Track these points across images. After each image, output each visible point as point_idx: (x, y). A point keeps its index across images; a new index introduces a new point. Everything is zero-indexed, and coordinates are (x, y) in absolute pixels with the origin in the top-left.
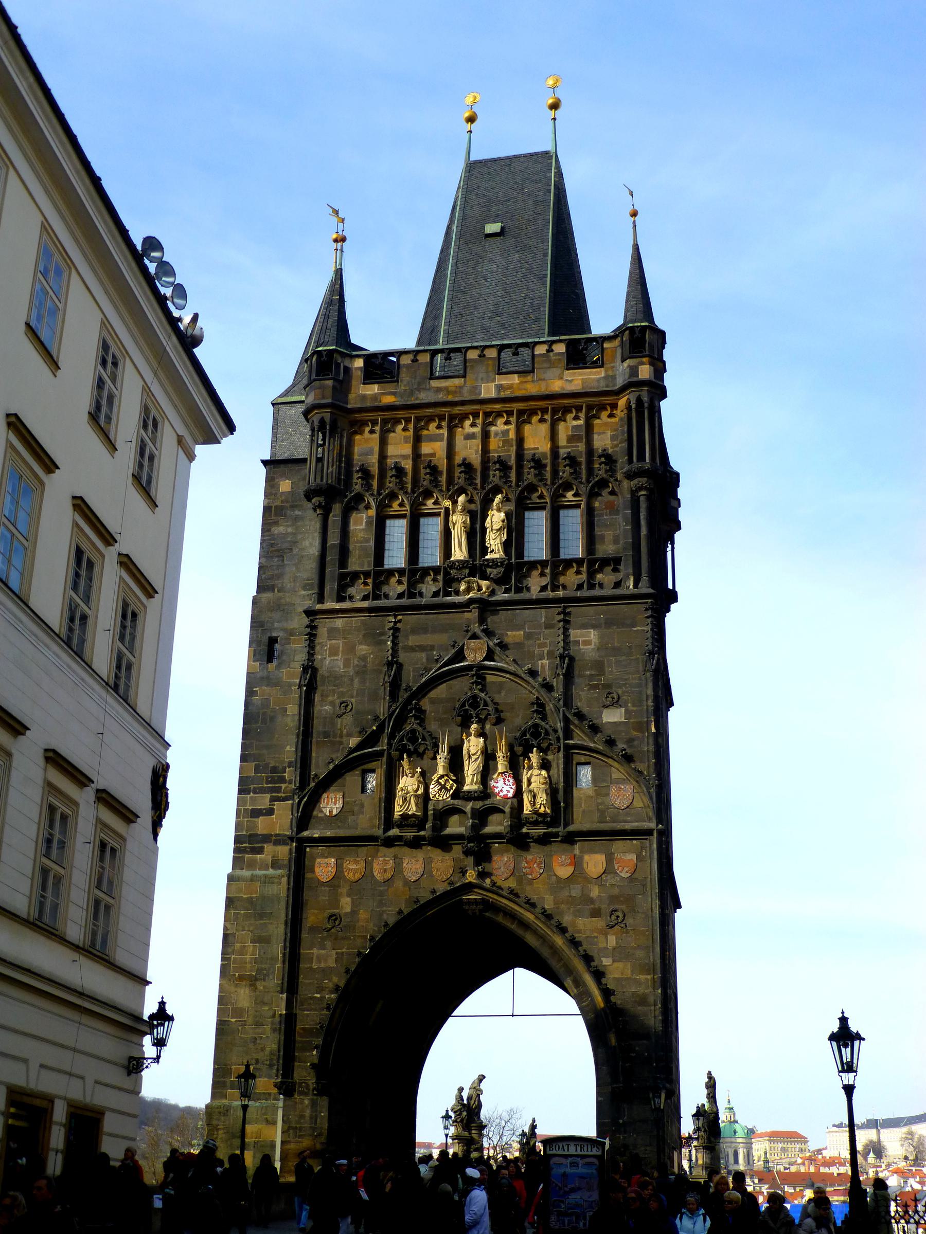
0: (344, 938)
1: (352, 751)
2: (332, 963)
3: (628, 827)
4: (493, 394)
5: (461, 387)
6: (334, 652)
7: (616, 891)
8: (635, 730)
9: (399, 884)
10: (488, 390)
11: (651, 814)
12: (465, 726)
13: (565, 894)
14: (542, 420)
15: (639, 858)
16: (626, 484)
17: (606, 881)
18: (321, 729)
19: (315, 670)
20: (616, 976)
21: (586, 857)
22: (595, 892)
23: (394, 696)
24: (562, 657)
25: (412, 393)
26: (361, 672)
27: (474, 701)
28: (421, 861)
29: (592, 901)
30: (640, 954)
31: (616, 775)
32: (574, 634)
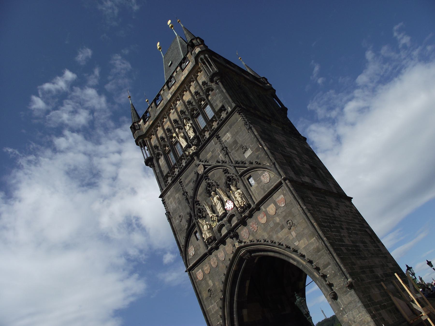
0: (216, 296)
1: (187, 229)
2: (217, 308)
3: (272, 187)
4: (171, 96)
5: (163, 103)
6: (171, 203)
7: (284, 214)
8: (257, 152)
9: (221, 264)
10: (169, 96)
11: (278, 176)
12: (210, 196)
13: (269, 228)
14: (186, 91)
15: (284, 195)
16: (213, 84)
17: (279, 212)
18: (179, 229)
19: (169, 213)
20: (303, 247)
21: (268, 209)
22: (278, 220)
23: (189, 203)
24: (223, 149)
25: (155, 116)
26: (180, 203)
27: (209, 185)
28: (223, 252)
29: (278, 224)
30: (306, 231)
31: (260, 172)
32: (223, 139)
